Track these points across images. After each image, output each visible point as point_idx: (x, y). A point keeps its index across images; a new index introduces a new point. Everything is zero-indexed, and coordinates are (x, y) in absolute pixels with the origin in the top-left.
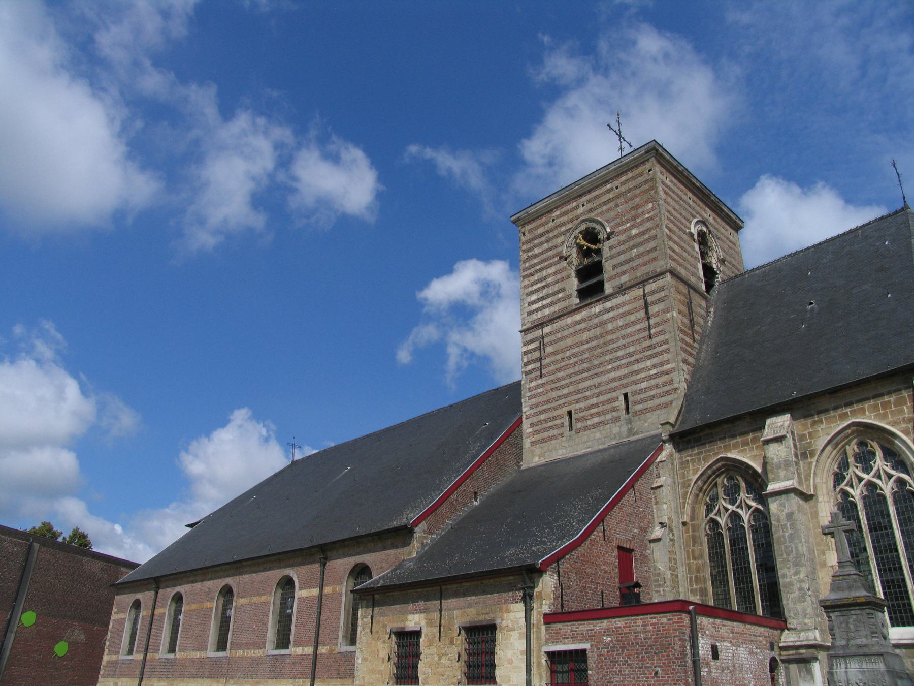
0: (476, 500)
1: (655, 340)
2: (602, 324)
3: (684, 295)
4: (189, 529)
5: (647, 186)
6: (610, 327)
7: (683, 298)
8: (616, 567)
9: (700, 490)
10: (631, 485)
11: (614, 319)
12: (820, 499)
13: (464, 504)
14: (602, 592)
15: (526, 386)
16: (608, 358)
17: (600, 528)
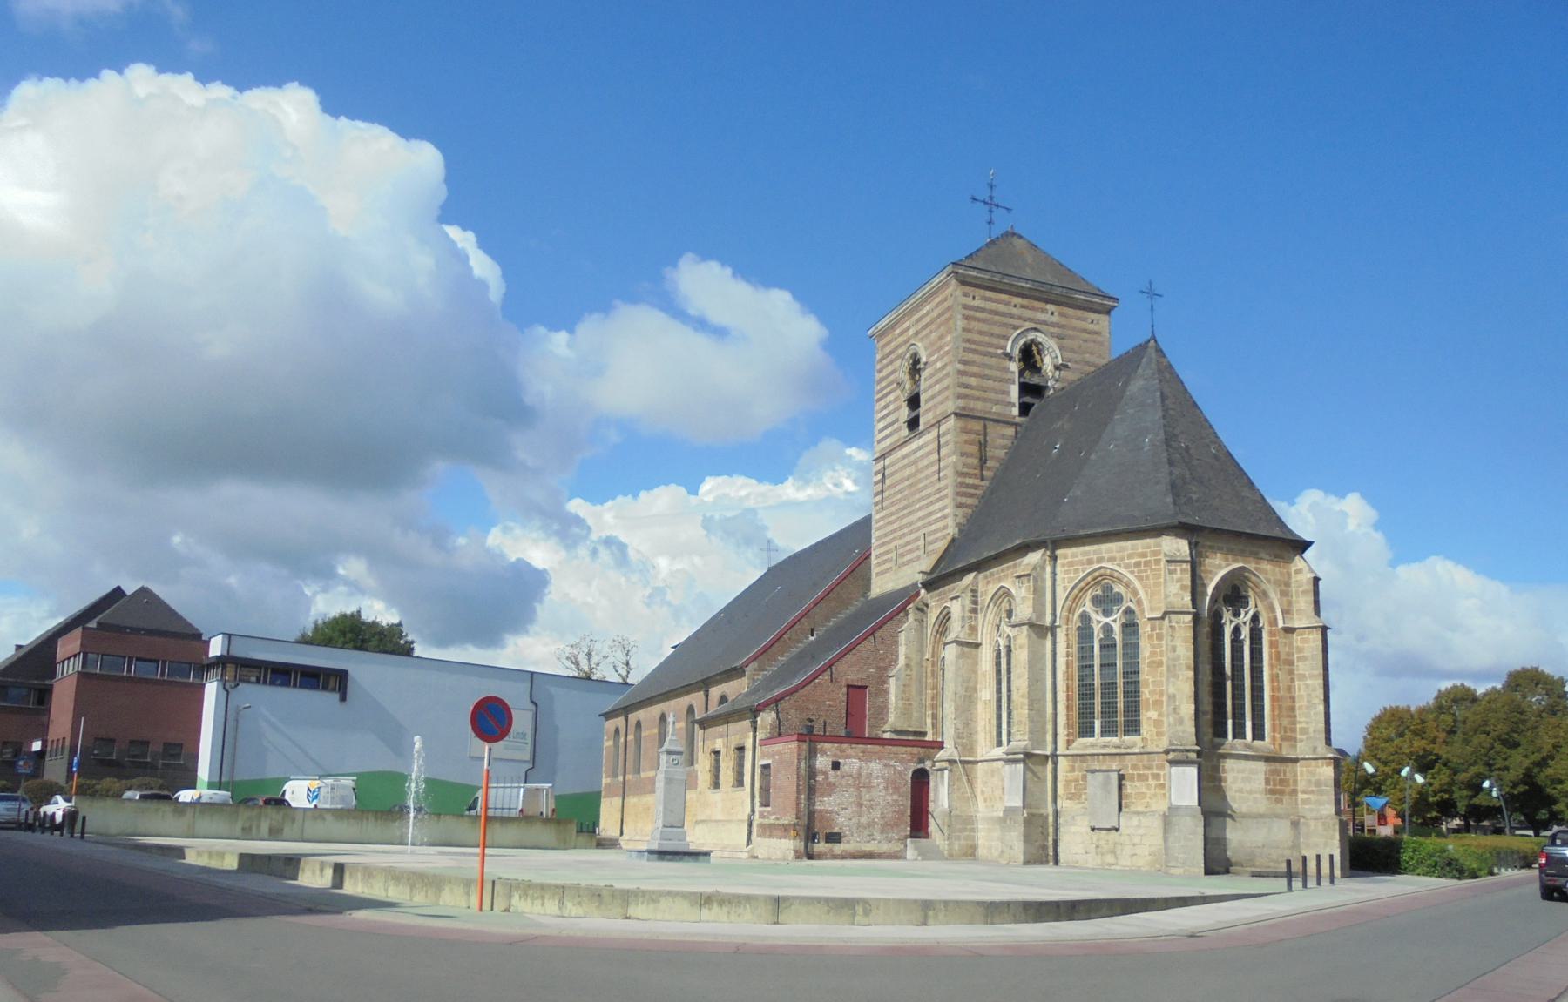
0: (812, 636)
1: (943, 483)
2: (915, 462)
3: (977, 433)
4: (674, 650)
5: (947, 315)
6: (920, 465)
7: (973, 436)
8: (843, 701)
9: (937, 632)
10: (872, 633)
11: (922, 457)
12: (984, 646)
13: (799, 641)
14: (825, 722)
15: (875, 517)
16: (917, 497)
17: (828, 672)
